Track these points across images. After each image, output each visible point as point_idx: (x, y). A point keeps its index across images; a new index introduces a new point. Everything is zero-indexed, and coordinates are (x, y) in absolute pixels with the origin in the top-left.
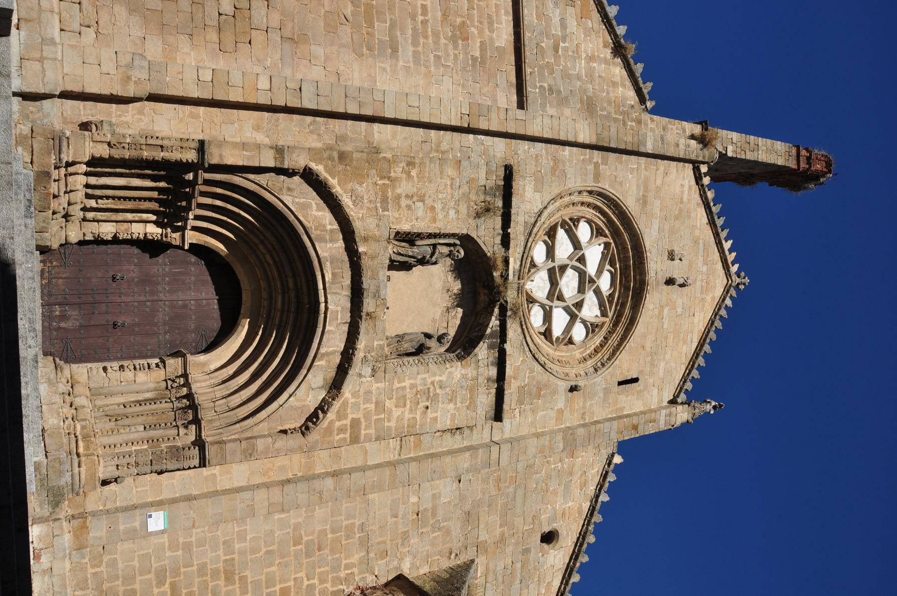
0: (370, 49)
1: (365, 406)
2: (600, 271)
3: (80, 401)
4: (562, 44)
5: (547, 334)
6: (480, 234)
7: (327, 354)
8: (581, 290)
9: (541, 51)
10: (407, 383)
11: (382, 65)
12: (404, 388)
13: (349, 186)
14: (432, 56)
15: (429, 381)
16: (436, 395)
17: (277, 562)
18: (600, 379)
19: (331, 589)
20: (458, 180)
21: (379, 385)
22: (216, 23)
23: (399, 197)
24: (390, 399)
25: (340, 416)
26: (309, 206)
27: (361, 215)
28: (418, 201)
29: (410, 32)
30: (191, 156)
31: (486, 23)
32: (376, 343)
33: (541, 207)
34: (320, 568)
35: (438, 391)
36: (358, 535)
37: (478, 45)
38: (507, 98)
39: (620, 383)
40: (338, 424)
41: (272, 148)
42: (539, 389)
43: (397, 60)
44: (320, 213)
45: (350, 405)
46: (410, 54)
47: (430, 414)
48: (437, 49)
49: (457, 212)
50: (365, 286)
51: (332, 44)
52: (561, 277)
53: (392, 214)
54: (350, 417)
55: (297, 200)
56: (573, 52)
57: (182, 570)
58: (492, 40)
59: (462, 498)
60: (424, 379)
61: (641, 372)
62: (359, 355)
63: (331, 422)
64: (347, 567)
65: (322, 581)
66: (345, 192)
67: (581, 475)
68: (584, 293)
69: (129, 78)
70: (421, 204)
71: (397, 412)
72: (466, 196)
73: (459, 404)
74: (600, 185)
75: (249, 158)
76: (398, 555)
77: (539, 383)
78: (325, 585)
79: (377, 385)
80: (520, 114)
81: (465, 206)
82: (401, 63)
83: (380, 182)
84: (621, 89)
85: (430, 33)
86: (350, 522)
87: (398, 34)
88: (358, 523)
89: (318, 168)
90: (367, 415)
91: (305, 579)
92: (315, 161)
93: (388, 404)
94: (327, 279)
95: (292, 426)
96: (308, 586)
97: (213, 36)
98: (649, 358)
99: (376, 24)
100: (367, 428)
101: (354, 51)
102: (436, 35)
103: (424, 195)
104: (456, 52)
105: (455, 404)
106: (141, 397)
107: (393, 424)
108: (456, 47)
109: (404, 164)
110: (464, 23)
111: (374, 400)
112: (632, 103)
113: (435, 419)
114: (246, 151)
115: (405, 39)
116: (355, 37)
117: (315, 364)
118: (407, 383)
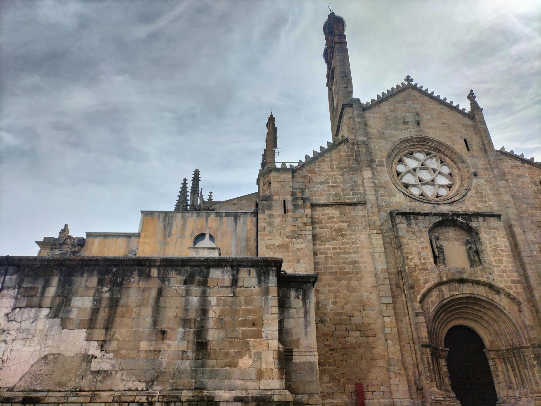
0: (357, 273)
2: (417, 159)
4: (331, 184)
5: (449, 187)
7: (486, 293)
8: (427, 169)
9: (337, 194)
10: (492, 259)
12: (495, 260)
13: (422, 284)
14: (353, 246)
15: (490, 249)
16: (495, 246)
18: (468, 161)
21: (495, 271)
22: (365, 338)
26: (432, 301)
29: (345, 255)
30: (428, 350)
31: (332, 220)
33: (402, 194)
35: (493, 244)
37: (342, 224)
38: (360, 211)
39: (468, 150)
40: (514, 290)
46: (355, 255)
47: (503, 248)
48: (349, 243)
49: (420, 237)
50: (459, 278)
51: (360, 289)
52: (424, 180)
54: (510, 284)
58: (338, 218)
59: (532, 230)
60: (489, 251)
61: (461, 138)
62: (485, 280)
63: (514, 292)
69: (399, 373)
70: (422, 254)
71: (505, 264)
72: (414, 233)
73: (497, 235)
75: (424, 327)
77: (476, 193)
80: (369, 206)
82: (360, 259)
83: (418, 272)
84: (341, 153)
89: (419, 297)
90: (509, 277)
92: (416, 299)
93: (502, 268)
95: (517, 309)
97: (371, 339)
99: (347, 270)
100: (513, 277)
101: (361, 280)
102: (343, 244)
106: (510, 370)
107: (510, 265)
108: (346, 235)
110: (335, 231)
113: (504, 245)
115: (349, 257)
116: (355, 279)
117: (490, 298)
118: (492, 259)
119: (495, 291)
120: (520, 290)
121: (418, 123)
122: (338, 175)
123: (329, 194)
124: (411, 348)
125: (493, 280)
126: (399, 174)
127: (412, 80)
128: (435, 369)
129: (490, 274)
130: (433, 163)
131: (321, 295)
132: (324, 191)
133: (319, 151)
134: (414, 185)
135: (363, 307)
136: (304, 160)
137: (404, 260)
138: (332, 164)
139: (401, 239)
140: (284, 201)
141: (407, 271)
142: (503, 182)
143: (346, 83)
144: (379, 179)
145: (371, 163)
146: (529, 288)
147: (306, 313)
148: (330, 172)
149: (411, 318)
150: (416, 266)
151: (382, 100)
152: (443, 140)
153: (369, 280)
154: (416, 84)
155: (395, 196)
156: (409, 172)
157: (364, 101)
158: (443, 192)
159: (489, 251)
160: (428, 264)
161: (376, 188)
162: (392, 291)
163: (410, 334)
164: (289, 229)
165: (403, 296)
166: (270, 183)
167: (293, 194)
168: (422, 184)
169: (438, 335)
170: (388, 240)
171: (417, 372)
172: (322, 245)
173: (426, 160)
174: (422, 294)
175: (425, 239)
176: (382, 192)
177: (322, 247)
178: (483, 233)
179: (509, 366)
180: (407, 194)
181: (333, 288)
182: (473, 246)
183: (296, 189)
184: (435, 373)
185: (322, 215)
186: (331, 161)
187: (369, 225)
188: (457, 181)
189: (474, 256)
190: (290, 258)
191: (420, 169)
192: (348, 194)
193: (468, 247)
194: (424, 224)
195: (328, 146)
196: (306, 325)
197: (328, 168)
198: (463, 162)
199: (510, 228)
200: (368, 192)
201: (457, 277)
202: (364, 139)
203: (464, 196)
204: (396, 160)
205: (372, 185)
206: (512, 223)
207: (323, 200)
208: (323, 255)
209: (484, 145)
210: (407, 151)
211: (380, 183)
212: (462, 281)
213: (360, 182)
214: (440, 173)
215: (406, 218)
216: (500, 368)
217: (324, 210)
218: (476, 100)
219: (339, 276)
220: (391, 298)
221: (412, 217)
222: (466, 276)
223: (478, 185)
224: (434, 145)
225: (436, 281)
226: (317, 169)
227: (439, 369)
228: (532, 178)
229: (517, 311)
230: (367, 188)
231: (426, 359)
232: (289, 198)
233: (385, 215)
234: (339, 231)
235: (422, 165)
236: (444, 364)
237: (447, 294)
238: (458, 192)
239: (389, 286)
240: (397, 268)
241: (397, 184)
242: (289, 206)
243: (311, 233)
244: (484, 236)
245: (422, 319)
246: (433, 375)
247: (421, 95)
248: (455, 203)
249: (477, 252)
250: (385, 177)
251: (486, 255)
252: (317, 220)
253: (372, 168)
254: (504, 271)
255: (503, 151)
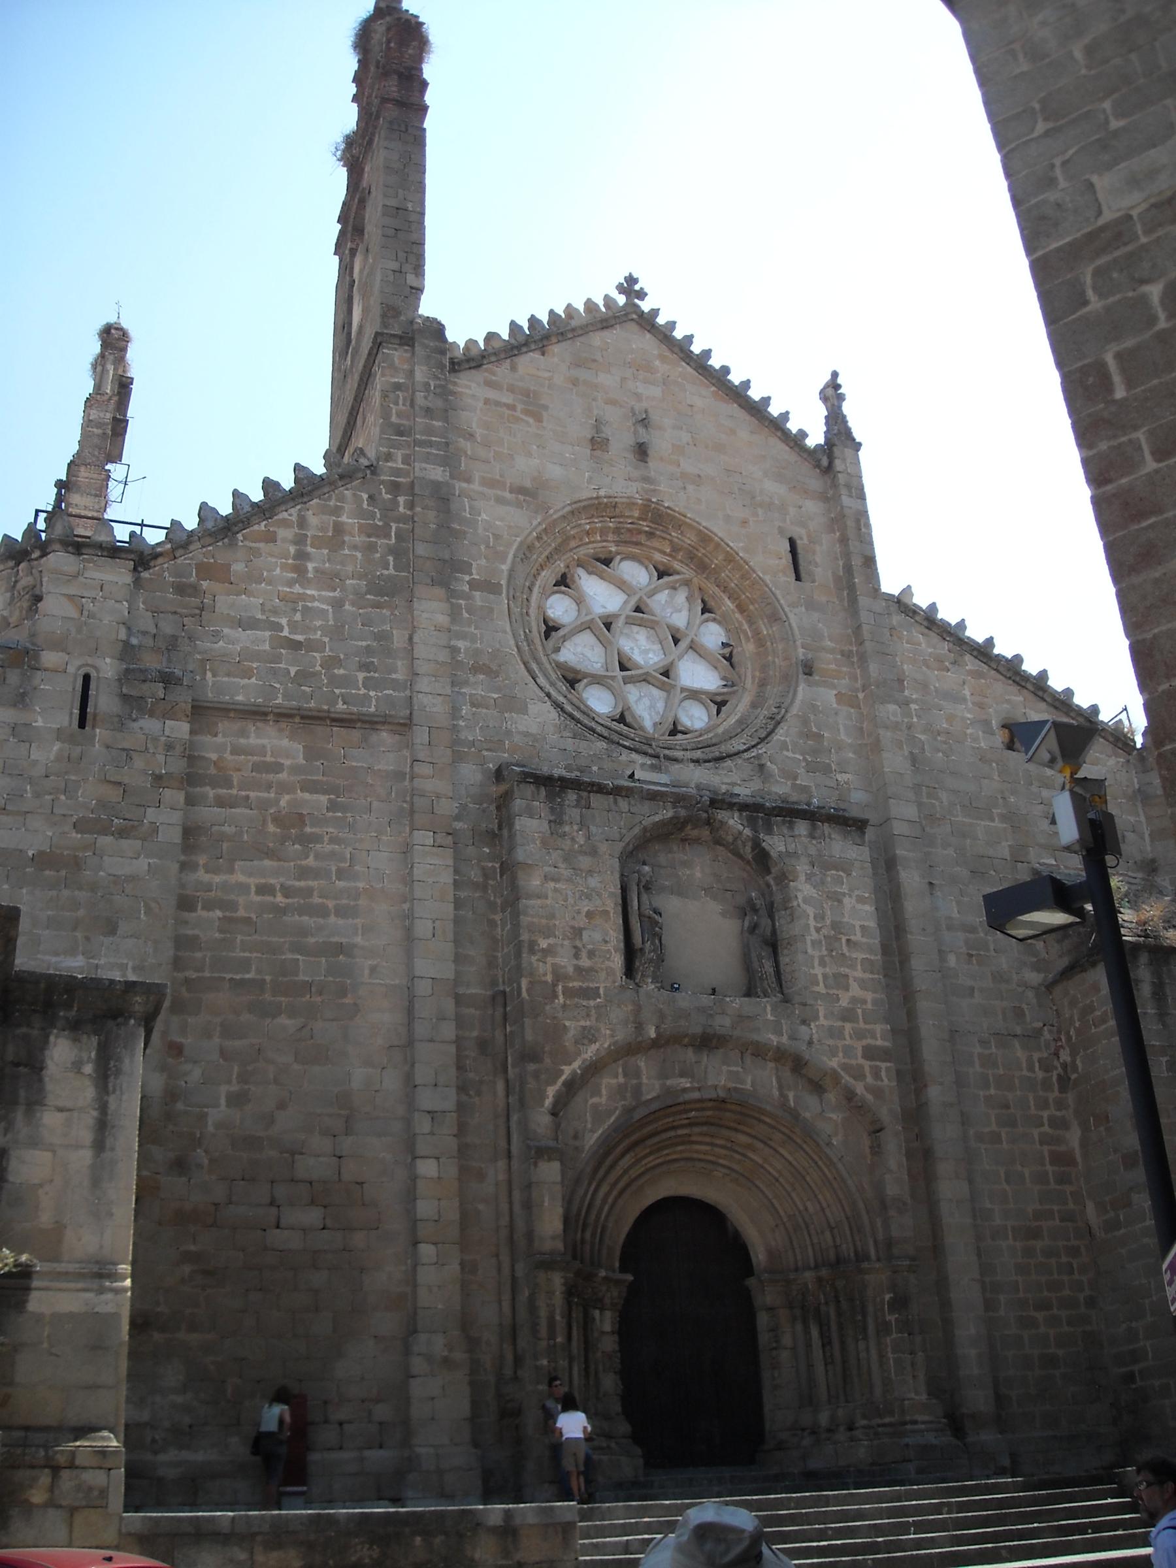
0: (343, 992)
1: (847, 1037)
2: (621, 585)
3: (824, 1418)
4: (286, 633)
5: (720, 703)
6: (617, 837)
7: (780, 1088)
8: (651, 625)
9: (304, 676)
10: (818, 971)
11: (367, 972)
12: (825, 976)
14: (341, 884)
15: (815, 936)
17: (1019, 1168)
18: (791, 616)
19: (1056, 1093)
20: (547, 869)
21: (821, 1014)
23: (578, 969)
24: (838, 999)
25: (859, 1075)
27: (608, 1032)
28: (581, 939)
31: (271, 776)
32: (769, 1017)
34: (1029, 1108)
36: (994, 1050)
37: (307, 796)
39: (798, 578)
40: (869, 1079)
41: (536, 1164)
42: (808, 735)
43: (355, 946)
44: (604, 1092)
45: (846, 1061)
46: (341, 922)
47: (857, 937)
49: (590, 872)
50: (698, 1030)
52: (638, 667)
53: (602, 984)
54: (861, 1061)
55: (589, 1126)
56: (295, 610)
57: (1021, 1295)
58: (295, 769)
60: (813, 943)
61: (781, 531)
64: (1031, 1069)
65: (1043, 1104)
66: (579, 1054)
67: (928, 667)
68: (657, 623)
69: (446, 1361)
70: (585, 934)
71: (855, 990)
72: (568, 858)
74: (503, 582)
76: (1020, 989)
78: (1051, 1101)
79: (822, 1018)
81: (581, 858)
82: (358, 940)
83: (561, 999)
85: (302, 884)
86: (976, 1059)
87: (312, 940)
88: (978, 1049)
89: (551, 1091)
91: (1042, 1129)
93: (844, 1003)
94: (688, 1085)
96: (1050, 1126)
97: (359, 1239)
98: (760, 511)
99: (302, 977)
100: (874, 1037)
102: (304, 873)
103: (573, 927)
104: (326, 839)
105: (844, 894)
107: (869, 996)
108: (317, 839)
109: (534, 958)
110: (276, 820)
111: (840, 1023)
112: (365, 496)
113: (862, 927)
114: (543, 1202)
119: (810, 1081)
120: (887, 1082)
121: (642, 451)
122: (321, 600)
123: (274, 672)
124: (499, 1270)
125: (810, 1043)
126: (550, 628)
127: (641, 295)
128: (574, 1343)
129: (804, 1022)
130: (674, 607)
131: (188, 1067)
132: (257, 656)
133: (257, 495)
134: (597, 680)
135: (348, 1119)
136: (191, 523)
137: (518, 955)
138: (302, 556)
139: (520, 874)
140: (87, 678)
141: (524, 994)
142: (892, 707)
143: (401, 255)
144: (473, 639)
145: (445, 574)
146: (912, 1077)
147: (103, 1126)
148: (290, 583)
149: (515, 1164)
150: (559, 976)
151: (526, 344)
152: (718, 528)
153: (380, 1018)
154: (655, 312)
155: (524, 710)
156: (588, 626)
157: (458, 334)
158: (696, 717)
159: (813, 943)
160: (603, 975)
161: (456, 670)
162: (460, 1068)
163: (504, 1221)
164: (89, 792)
165: (500, 1086)
166: (38, 599)
167: (127, 651)
168: (626, 681)
169: (604, 1228)
170: (475, 875)
171: (509, 1357)
172: (216, 871)
173: (651, 594)
174: (565, 1084)
175: (605, 886)
176: (478, 686)
177: (217, 879)
178: (802, 878)
179: (815, 1333)
180: (569, 708)
181: (238, 1043)
182: (765, 922)
183: (145, 633)
184: (571, 1360)
185: (236, 751)
186: (300, 540)
187: (412, 812)
188: (749, 683)
189: (760, 958)
190: (81, 913)
191: (630, 622)
192: (346, 682)
193: (746, 924)
194: (611, 826)
195: (297, 480)
196: (98, 1176)
197: (284, 567)
198: (775, 617)
199: (887, 865)
200: (423, 684)
201: (695, 1028)
202: (437, 473)
203: (762, 740)
204: (548, 576)
205: (443, 656)
206: (899, 852)
207: (244, 690)
208: (219, 913)
209: (848, 569)
210: (589, 550)
211: (477, 653)
212: (708, 1042)
213: (399, 639)
214: (693, 647)
215: (550, 797)
216: (787, 1340)
217: (243, 733)
218: (846, 408)
219: (268, 997)
220: (452, 1092)
221: (571, 796)
222: (722, 1024)
223: (814, 708)
224: (690, 539)
225: (623, 1035)
226: (238, 567)
227: (588, 1346)
228: (981, 706)
229: (868, 1150)
230: (422, 668)
231: (543, 1313)
232: (108, 668)
233: (479, 777)
234: (294, 821)
235: (638, 609)
236: (607, 1327)
237: (651, 1087)
238: (743, 723)
239: (452, 1049)
240: (494, 983)
241: (539, 663)
242: (104, 702)
243: (176, 817)
244: (803, 890)
245: (550, 1171)
246: (563, 1363)
247: (668, 354)
248: (729, 763)
249: (773, 945)
250: (499, 635)
251: (800, 957)
252: (213, 771)
253: (452, 594)
254: (847, 1016)
255: (905, 600)
